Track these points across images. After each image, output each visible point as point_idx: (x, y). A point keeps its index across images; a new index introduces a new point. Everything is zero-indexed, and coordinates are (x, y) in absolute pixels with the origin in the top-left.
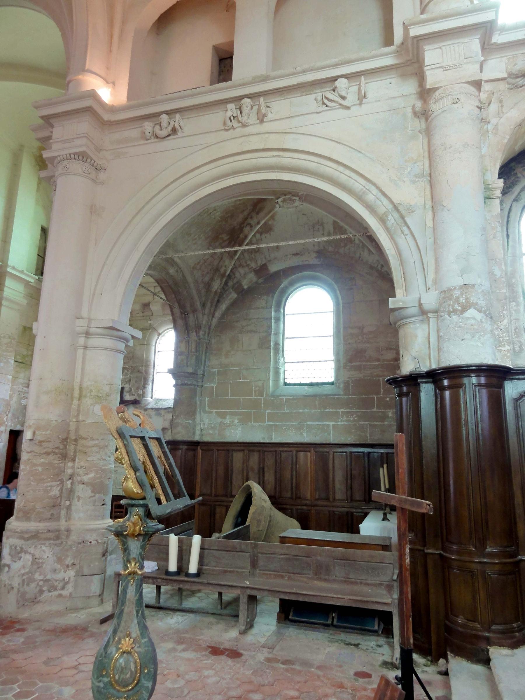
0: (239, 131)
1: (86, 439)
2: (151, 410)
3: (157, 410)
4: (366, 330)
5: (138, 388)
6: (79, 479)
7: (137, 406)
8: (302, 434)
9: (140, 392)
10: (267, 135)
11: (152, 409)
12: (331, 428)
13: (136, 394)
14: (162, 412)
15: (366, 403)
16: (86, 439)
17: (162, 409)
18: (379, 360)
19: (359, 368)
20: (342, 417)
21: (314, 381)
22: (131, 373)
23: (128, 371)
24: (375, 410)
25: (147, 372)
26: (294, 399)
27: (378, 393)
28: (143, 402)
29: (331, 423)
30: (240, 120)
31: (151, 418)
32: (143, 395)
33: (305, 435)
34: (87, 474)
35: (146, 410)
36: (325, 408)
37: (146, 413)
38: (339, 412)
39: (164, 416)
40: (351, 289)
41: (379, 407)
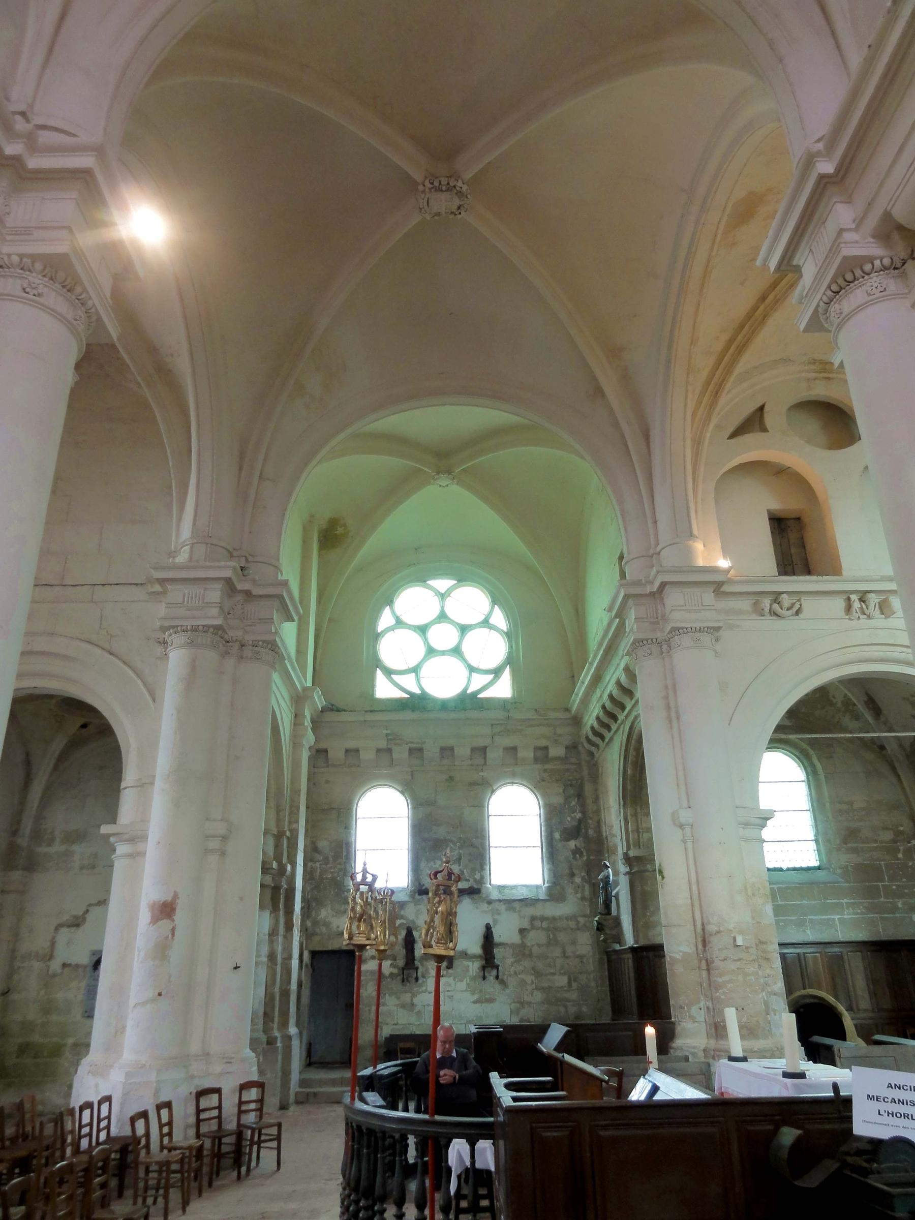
0: (864, 621)
1: (766, 943)
2: (497, 903)
3: (510, 903)
4: (856, 806)
5: (473, 870)
6: (769, 989)
7: (476, 896)
8: (804, 931)
9: (477, 876)
10: (895, 631)
11: (500, 901)
12: (837, 922)
13: (472, 880)
14: (516, 905)
15: (871, 893)
16: (766, 943)
17: (515, 900)
18: (876, 841)
19: (855, 851)
20: (848, 908)
21: (798, 865)
22: (460, 848)
23: (455, 844)
24: (882, 899)
25: (484, 848)
26: (787, 888)
27: (883, 880)
28: (483, 891)
29: (837, 917)
30: (867, 612)
31: (499, 914)
32: (481, 881)
33: (808, 932)
34: (775, 983)
35: (490, 902)
36: (826, 899)
38: (842, 904)
39: (520, 911)
40: (831, 757)
41: (886, 897)
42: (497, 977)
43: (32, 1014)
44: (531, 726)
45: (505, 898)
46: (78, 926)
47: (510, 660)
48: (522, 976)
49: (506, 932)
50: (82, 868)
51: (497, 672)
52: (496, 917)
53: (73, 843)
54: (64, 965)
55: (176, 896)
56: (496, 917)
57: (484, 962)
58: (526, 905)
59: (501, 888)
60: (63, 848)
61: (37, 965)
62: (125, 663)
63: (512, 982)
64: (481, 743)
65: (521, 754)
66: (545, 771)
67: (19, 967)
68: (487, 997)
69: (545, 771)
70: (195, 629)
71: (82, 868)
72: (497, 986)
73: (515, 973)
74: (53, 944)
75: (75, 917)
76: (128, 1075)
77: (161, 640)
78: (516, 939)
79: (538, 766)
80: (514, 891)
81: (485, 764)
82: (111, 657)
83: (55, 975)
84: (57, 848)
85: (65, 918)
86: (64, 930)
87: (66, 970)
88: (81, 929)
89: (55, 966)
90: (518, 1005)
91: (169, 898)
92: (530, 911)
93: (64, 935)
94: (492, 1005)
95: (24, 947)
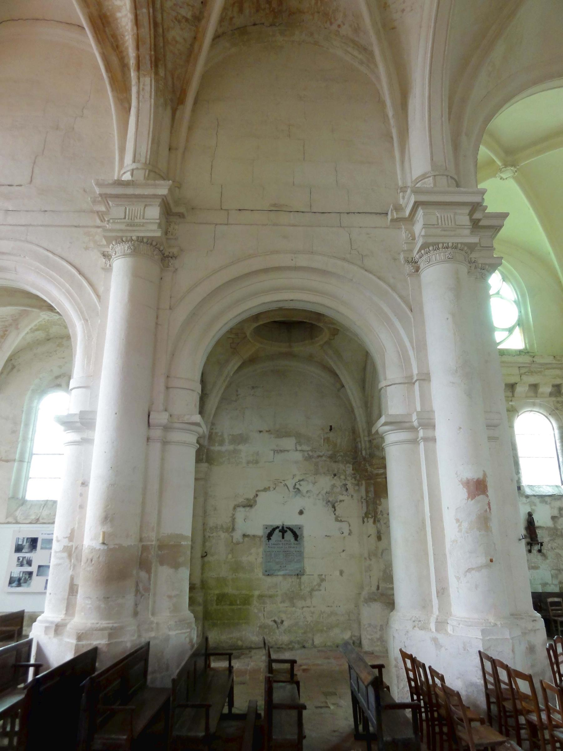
2: (533, 498)
3: (542, 497)
14: (548, 499)
31: (535, 505)
35: (527, 497)
37: (528, 500)
39: (550, 503)
42: (540, 551)
43: (224, 572)
44: (548, 369)
45: (535, 494)
46: (251, 506)
47: (520, 323)
48: (557, 551)
49: (542, 518)
50: (248, 463)
51: (511, 330)
52: (533, 507)
53: (239, 444)
54: (244, 536)
55: (485, 475)
56: (533, 507)
57: (529, 540)
58: (555, 499)
59: (530, 487)
60: (231, 447)
61: (223, 535)
62: (379, 278)
63: (550, 554)
64: (512, 380)
65: (541, 390)
66: (558, 402)
67: (209, 537)
68: (533, 565)
69: (558, 402)
70: (455, 247)
71: (248, 463)
72: (539, 556)
73: (552, 548)
74: (233, 520)
75: (248, 500)
76: (483, 632)
77: (410, 259)
78: (550, 524)
79: (554, 399)
80: (541, 489)
81: (513, 396)
82: (367, 273)
83: (238, 543)
84: (227, 447)
85: (240, 500)
86: (242, 509)
87: (246, 539)
88: (253, 510)
89: (237, 535)
90: (556, 572)
91: (477, 475)
92: (558, 504)
93: (241, 513)
94: (538, 571)
95: (211, 522)
